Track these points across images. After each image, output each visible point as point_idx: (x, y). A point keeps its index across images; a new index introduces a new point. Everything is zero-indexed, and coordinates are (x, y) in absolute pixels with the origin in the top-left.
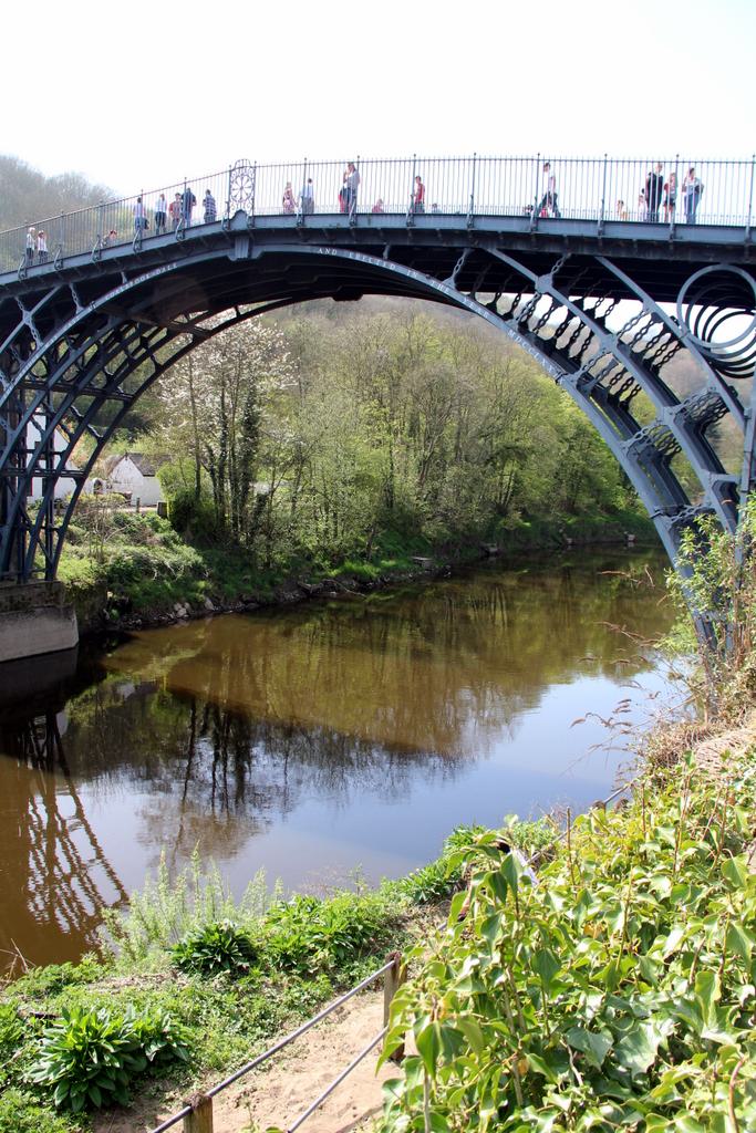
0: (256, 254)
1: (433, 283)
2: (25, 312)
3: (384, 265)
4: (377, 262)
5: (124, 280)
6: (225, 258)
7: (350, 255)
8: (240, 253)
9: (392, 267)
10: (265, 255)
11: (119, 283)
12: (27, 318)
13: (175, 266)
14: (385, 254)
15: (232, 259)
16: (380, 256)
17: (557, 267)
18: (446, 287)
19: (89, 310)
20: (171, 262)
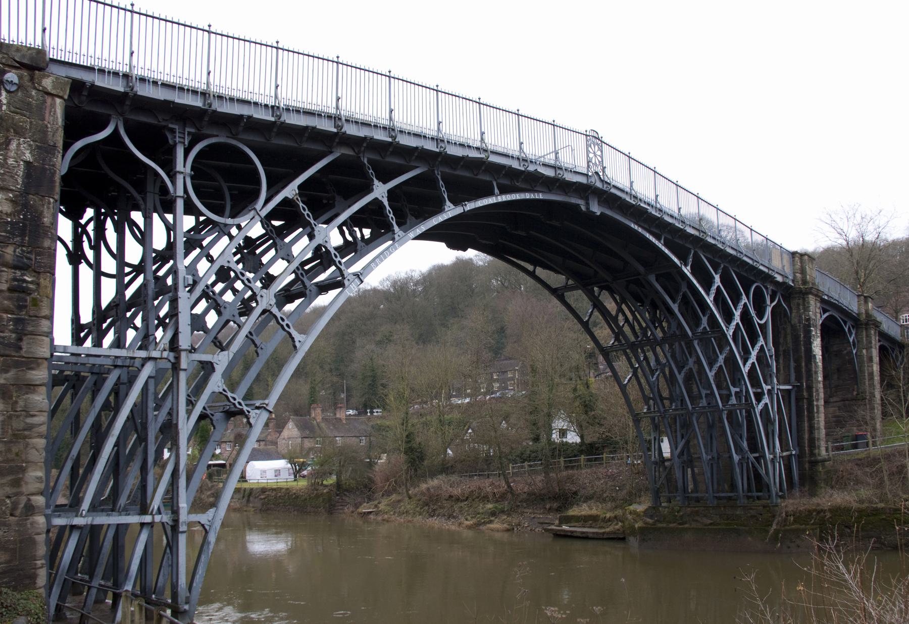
1: (683, 267)
2: (376, 182)
3: (663, 248)
4: (660, 246)
5: (496, 191)
7: (647, 235)
8: (596, 209)
9: (667, 251)
10: (602, 213)
11: (491, 193)
12: (380, 191)
13: (540, 196)
14: (662, 242)
15: (583, 208)
16: (659, 239)
19: (459, 210)
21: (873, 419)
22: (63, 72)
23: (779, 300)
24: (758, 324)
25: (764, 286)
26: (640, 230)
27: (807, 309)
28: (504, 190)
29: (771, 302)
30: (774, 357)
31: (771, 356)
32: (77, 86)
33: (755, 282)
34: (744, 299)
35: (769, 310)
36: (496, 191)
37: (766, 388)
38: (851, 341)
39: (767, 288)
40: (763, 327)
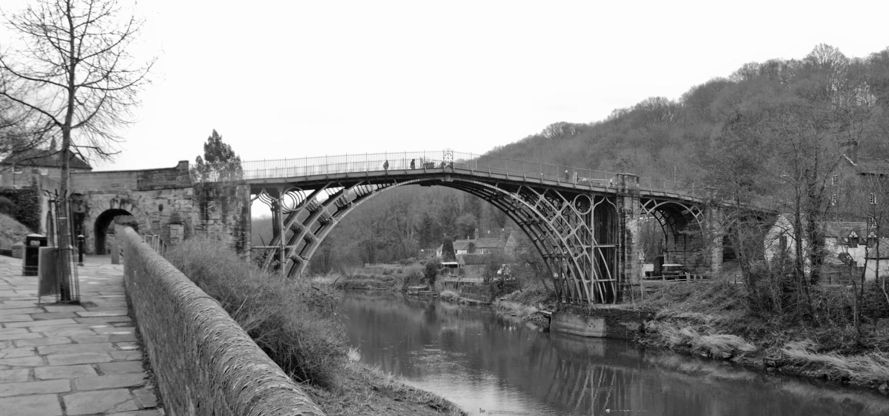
0: (452, 181)
3: (497, 189)
4: (494, 188)
8: (449, 179)
9: (499, 189)
14: (497, 186)
15: (443, 180)
16: (494, 184)
17: (545, 192)
18: (515, 196)
20: (417, 179)
21: (711, 263)
22: (249, 182)
23: (605, 199)
24: (582, 216)
25: (589, 196)
26: (480, 183)
27: (623, 203)
28: (398, 182)
29: (595, 203)
30: (593, 231)
31: (591, 231)
32: (252, 185)
33: (578, 194)
35: (592, 208)
36: (396, 182)
37: (584, 247)
38: (696, 216)
39: (589, 196)
40: (588, 217)
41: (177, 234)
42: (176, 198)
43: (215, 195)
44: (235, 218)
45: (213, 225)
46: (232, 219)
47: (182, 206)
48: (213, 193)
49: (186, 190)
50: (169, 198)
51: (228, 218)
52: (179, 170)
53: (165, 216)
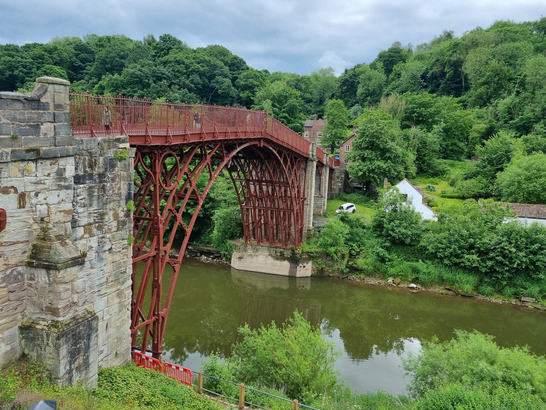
6: (257, 145)
8: (262, 144)
16: (275, 150)
28: (239, 146)
34: (295, 168)
41: (74, 291)
42: (40, 187)
43: (88, 169)
44: (116, 216)
45: (82, 238)
46: (112, 218)
47: (53, 209)
48: (85, 167)
49: (62, 162)
50: (21, 190)
51: (106, 218)
52: (45, 107)
53: (13, 244)
